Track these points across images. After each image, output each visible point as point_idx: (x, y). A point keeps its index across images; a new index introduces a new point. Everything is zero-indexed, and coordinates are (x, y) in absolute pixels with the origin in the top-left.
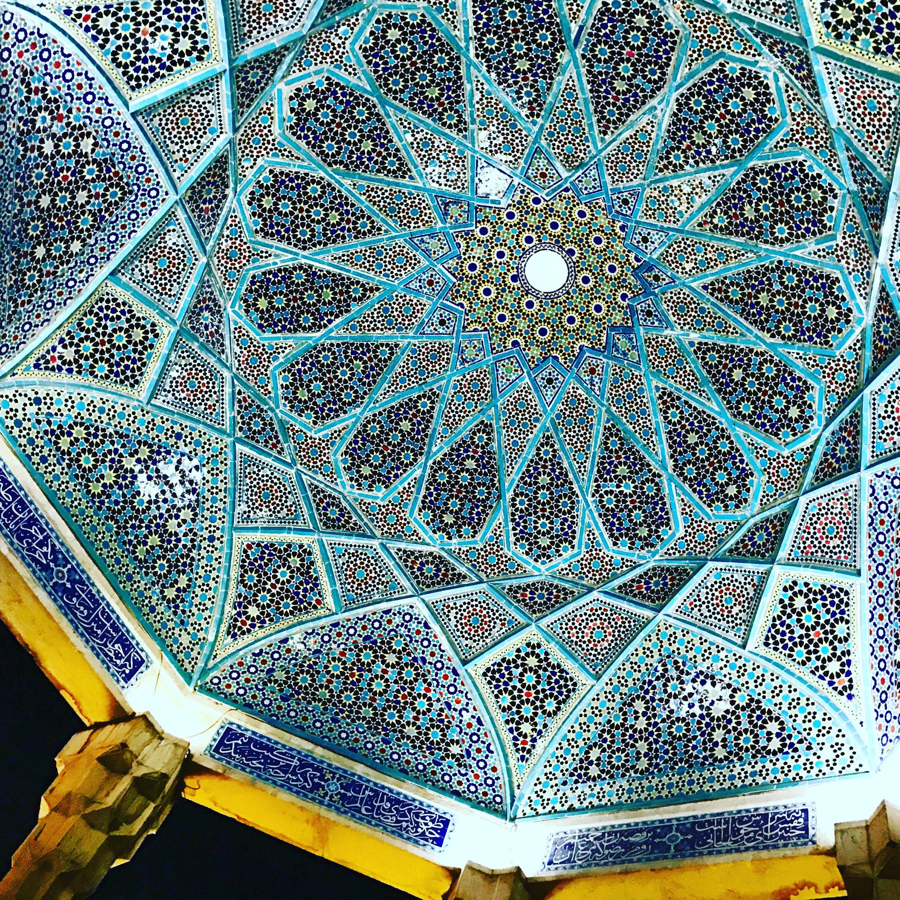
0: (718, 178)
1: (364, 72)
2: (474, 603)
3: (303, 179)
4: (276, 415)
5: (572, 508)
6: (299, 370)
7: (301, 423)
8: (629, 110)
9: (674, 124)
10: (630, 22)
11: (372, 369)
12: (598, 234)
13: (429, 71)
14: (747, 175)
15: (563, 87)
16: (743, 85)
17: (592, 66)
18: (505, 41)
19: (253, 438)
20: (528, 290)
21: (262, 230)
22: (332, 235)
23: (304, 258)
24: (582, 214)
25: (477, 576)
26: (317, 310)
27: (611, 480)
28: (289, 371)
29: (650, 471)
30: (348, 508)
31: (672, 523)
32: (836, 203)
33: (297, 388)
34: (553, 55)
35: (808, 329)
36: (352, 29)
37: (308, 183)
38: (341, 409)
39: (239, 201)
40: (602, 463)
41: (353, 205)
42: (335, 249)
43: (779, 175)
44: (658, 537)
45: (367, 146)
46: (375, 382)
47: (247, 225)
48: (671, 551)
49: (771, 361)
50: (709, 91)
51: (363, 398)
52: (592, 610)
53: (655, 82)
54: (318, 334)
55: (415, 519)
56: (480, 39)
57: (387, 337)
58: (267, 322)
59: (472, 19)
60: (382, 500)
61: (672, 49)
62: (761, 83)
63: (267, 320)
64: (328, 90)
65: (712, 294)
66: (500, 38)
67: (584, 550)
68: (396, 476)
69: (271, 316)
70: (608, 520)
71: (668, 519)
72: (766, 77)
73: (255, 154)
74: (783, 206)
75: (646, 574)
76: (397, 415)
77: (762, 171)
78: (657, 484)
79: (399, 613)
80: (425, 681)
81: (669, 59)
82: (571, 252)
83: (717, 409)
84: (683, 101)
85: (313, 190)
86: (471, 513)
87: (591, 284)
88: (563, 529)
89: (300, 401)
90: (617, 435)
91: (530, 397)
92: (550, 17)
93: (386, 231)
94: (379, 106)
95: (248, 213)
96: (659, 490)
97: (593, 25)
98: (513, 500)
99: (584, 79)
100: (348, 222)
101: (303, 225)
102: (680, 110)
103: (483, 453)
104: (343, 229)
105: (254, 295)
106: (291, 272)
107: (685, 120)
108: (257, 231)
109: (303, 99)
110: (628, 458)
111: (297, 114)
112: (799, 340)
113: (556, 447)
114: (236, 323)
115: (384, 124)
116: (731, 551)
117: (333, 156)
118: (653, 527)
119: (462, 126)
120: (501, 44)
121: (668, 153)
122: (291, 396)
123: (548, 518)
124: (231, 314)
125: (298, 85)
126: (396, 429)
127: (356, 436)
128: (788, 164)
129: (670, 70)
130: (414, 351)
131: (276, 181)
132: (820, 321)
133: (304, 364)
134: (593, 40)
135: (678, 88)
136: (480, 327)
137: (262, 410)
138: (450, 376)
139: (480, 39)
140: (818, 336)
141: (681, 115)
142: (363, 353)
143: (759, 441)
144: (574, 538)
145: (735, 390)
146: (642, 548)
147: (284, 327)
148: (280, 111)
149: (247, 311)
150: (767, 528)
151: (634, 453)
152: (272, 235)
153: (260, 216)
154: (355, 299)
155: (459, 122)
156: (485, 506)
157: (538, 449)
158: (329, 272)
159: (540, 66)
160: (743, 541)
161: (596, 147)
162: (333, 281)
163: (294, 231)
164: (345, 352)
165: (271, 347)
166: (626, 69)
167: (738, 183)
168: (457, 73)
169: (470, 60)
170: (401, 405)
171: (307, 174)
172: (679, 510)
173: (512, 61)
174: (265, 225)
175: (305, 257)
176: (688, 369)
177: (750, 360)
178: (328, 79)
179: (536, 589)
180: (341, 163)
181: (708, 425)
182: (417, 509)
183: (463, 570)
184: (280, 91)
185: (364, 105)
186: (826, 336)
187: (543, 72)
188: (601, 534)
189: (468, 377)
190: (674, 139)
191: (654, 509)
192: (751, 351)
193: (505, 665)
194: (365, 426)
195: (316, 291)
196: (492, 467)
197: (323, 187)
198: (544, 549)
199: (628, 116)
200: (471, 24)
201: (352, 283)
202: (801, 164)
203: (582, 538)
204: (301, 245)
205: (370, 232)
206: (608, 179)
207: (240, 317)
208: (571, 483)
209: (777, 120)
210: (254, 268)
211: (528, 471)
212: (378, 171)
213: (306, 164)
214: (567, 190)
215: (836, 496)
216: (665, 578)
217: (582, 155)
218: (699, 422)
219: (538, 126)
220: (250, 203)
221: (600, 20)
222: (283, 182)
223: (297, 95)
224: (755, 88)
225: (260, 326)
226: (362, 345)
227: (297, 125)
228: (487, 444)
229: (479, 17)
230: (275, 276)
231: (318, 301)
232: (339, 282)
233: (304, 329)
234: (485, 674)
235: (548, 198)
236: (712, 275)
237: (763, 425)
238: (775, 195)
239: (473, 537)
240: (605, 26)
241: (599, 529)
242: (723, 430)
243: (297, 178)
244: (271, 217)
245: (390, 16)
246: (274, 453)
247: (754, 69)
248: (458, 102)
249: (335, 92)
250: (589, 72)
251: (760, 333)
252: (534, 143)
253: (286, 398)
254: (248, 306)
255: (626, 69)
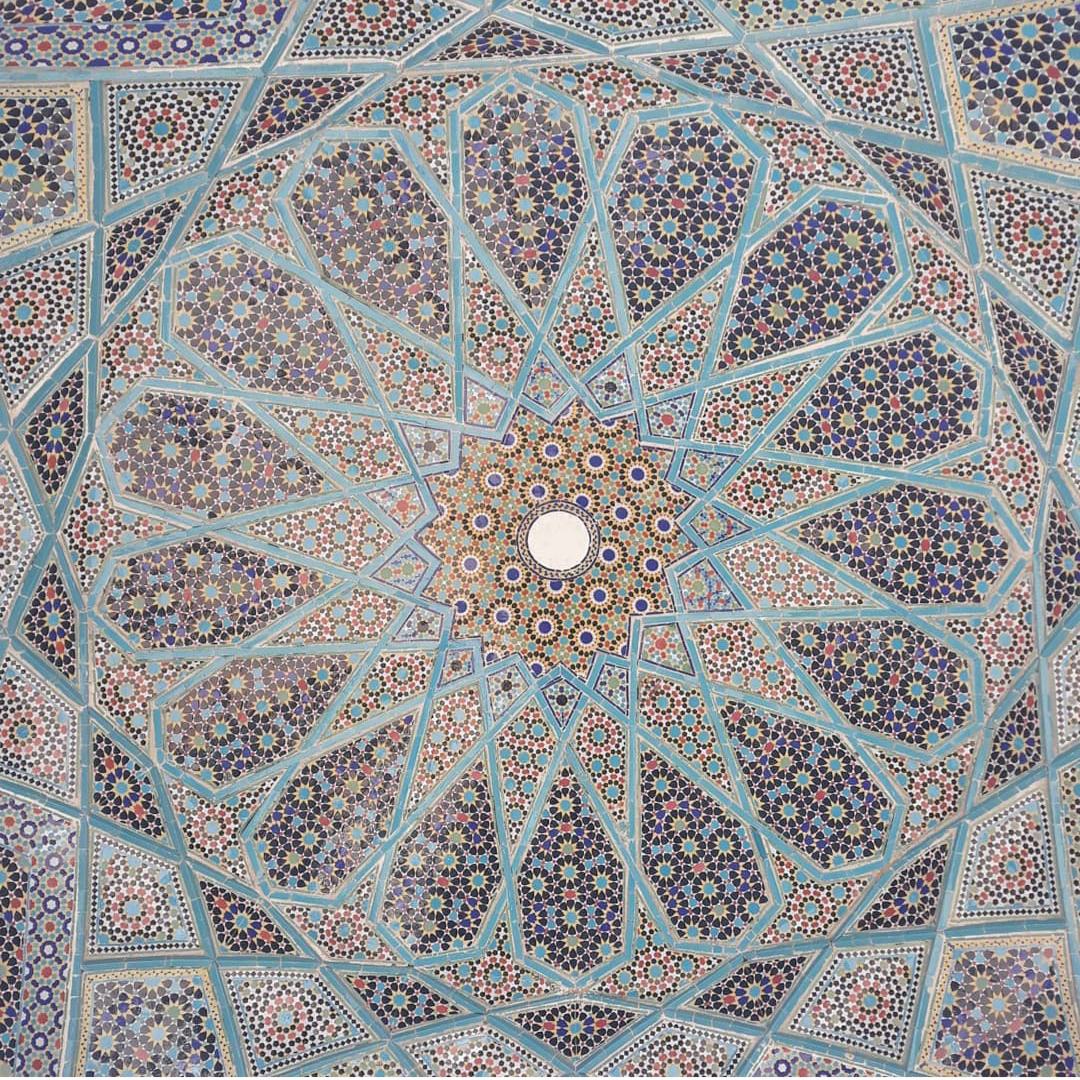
0: (514, 833)
1: (941, 635)
2: (192, 143)
3: (921, 447)
4: (704, 93)
5: (239, 369)
6: (731, 185)
7: (662, 114)
8: (649, 807)
9: (600, 837)
10: (728, 901)
11: (639, 262)
12: (551, 634)
13: (871, 683)
14: (496, 867)
15: (728, 770)
16: (585, 944)
17: (721, 820)
18: (822, 777)
19: (712, 54)
20: (556, 504)
21: (927, 344)
22: (831, 395)
23: (844, 342)
24: (587, 638)
25: (231, 169)
26: (774, 283)
27: (244, 443)
28: (743, 174)
29: (226, 506)
30: (484, 59)
31: (134, 496)
32: (408, 943)
33: (713, 157)
34: (765, 799)
35: (289, 819)
36: (990, 681)
37: (911, 445)
38: (629, 179)
39: (984, 363)
40: (276, 445)
41: (836, 452)
42: (815, 381)
43: (473, 903)
44: (124, 465)
45: (874, 540)
46: (620, 250)
47: (952, 339)
48: (93, 474)
49: (277, 749)
50: (604, 906)
51: (616, 217)
52: (69, 318)
53: (654, 863)
54: (746, 254)
55: (386, 134)
56: (847, 760)
57: (659, 316)
58: (828, 218)
59: (873, 778)
60: (453, 114)
61: (670, 912)
62: (573, 963)
63: (830, 221)
64: (968, 585)
65: (396, 723)
66: (829, 777)
67: (167, 345)
68: (470, 160)
69: (828, 231)
70: (190, 408)
71: (144, 494)
72: (575, 974)
73: (1004, 445)
74: (440, 881)
75: (79, 419)
76: (552, 234)
77: (489, 887)
78: (201, 506)
79: (265, 31)
80: (118, 14)
81: (665, 899)
82: (556, 586)
83: (257, 646)
84: (616, 870)
85: (898, 441)
86: (332, 218)
87: (504, 577)
88: (217, 334)
89: (692, 142)
90: (301, 487)
91: (430, 409)
92: (800, 838)
93: (772, 445)
94: (897, 602)
95: (961, 355)
96: (193, 504)
97: (756, 868)
98: (307, 293)
99: (716, 799)
100: (826, 427)
101: (879, 385)
102: (609, 857)
103: (404, 299)
104: (825, 413)
105: (874, 245)
106: (847, 310)
107: (596, 853)
108: (932, 337)
109: (990, 553)
110: (261, 484)
111: (985, 530)
112: (283, 801)
113: (339, 398)
114: (870, 186)
115: (875, 582)
116: (54, 569)
117: (905, 501)
118: (143, 465)
119: (789, 639)
120: (823, 770)
121: (577, 801)
122: (711, 140)
123: (247, 323)
124: (886, 195)
125: (1007, 570)
126: (534, 216)
127: (575, 159)
128: (478, 922)
129: (654, 888)
130: (612, 327)
131: (953, 422)
132: (290, 840)
133: (731, 198)
134: (743, 851)
135: (632, 881)
136: (564, 418)
137: (734, 90)
138: (539, 337)
139: (847, 760)
140: (274, 828)
141: (603, 854)
142: (669, 273)
143: (186, 676)
144: (194, 344)
145: (267, 681)
146: (120, 431)
147: (800, 228)
148: (1008, 522)
149: (866, 215)
150: (62, 635)
151: (263, 496)
152: (909, 346)
153: (942, 362)
154: (739, 332)
155: (796, 643)
156: (327, 245)
157: (354, 373)
158: (799, 344)
159: (767, 775)
160: (59, 590)
161: (642, 732)
162: (785, 336)
163: (884, 370)
164: (692, 256)
165: (796, 188)
166: (690, 847)
167: (494, 851)
168: (842, 701)
169: (840, 729)
170: (559, 251)
171: (921, 456)
172: (154, 517)
173: (797, 757)
174: (927, 353)
175: (846, 344)
176: (328, 636)
177: (293, 723)
178: (977, 599)
179: (150, 242)
180: (890, 499)
181: (242, 620)
182: (399, 148)
183: (253, 152)
184: (1025, 547)
185: (914, 592)
186: (270, 837)
187: (759, 771)
188: (175, 385)
189: (520, 355)
190: (586, 820)
191: (169, 481)
192: (304, 731)
193: (60, 143)
194: (577, 184)
195: (795, 307)
196: (375, 296)
197: (889, 453)
198: (204, 289)
199: (646, 800)
200: (870, 772)
201: (759, 350)
202: (469, 937)
203: (185, 350)
204: (862, 356)
205: (790, 432)
206: (601, 708)
207: (870, 199)
208: (276, 388)
209: (528, 948)
210: (902, 281)
211: (334, 339)
212: (838, 515)
213: (931, 470)
214: (625, 650)
215: (67, 760)
216: (59, 449)
217: (646, 709)
218: (253, 611)
219: (714, 701)
220: (967, 369)
221: (754, 879)
222: (944, 428)
223: (1000, 554)
224: (573, 954)
225: (832, 207)
226: (680, 282)
227: (976, 516)
228: (412, 313)
229: (866, 785)
230: (864, 291)
231: (782, 296)
232: (777, 340)
233: (771, 247)
234: (62, 103)
235: (633, 619)
236: (418, 739)
237: (203, 694)
238: (456, 882)
239: (295, 197)
240: (745, 875)
241: (184, 386)
242: (224, 637)
243: (930, 444)
244: (927, 368)
245: (959, 722)
246: (664, 55)
247: (591, 971)
248: (815, 666)
249: (958, 586)
250: (718, 811)
251: (318, 755)
252: (701, 675)
253: (714, 132)
254: (870, 224)
255: (690, 847)
